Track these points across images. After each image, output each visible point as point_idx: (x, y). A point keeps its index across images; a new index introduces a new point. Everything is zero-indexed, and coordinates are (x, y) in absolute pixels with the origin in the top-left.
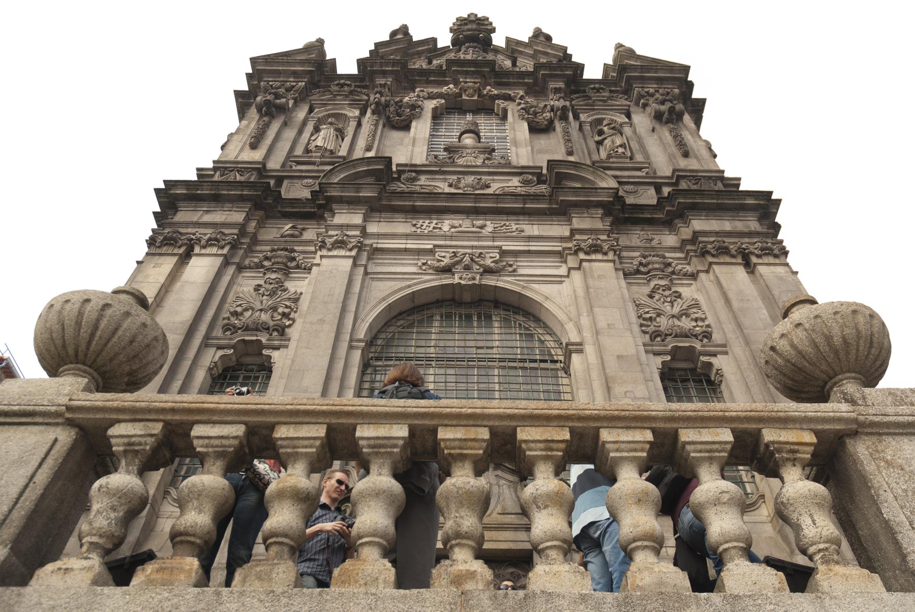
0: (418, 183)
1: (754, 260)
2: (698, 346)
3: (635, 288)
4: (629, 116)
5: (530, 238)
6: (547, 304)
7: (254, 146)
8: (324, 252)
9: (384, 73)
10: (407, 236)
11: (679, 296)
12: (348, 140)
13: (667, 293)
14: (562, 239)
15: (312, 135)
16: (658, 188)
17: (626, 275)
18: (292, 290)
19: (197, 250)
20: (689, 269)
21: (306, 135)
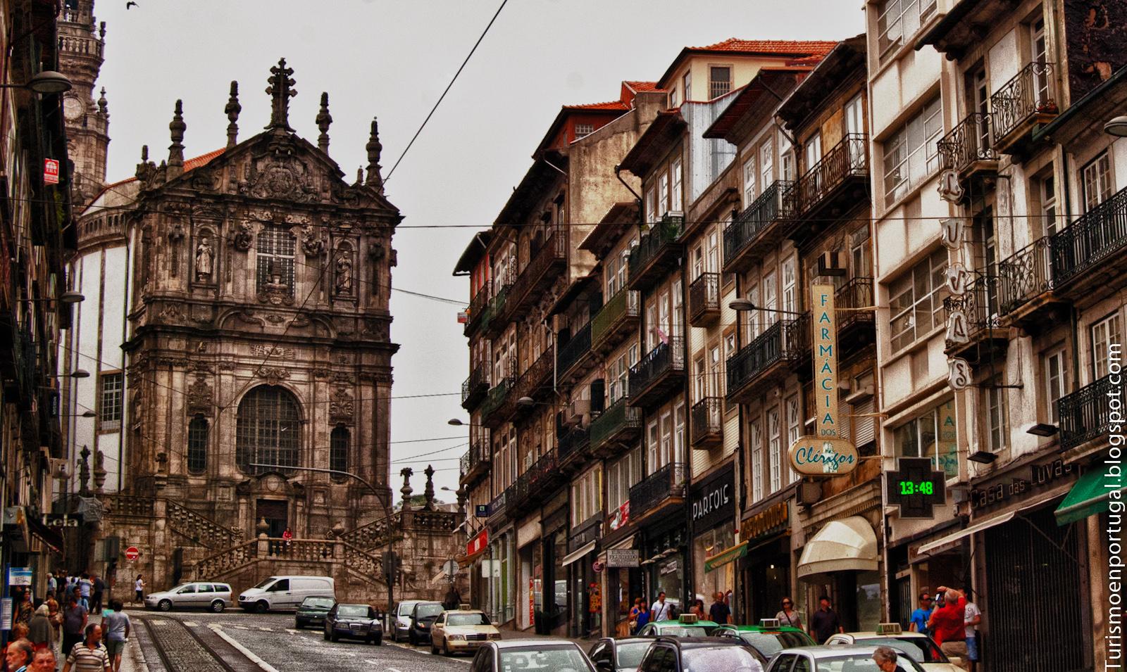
0: (254, 316)
1: (378, 384)
2: (346, 423)
3: (332, 389)
4: (358, 239)
5: (298, 361)
6: (300, 398)
7: (174, 276)
8: (222, 372)
9: (233, 203)
10: (250, 357)
11: (346, 394)
12: (215, 260)
13: (343, 394)
14: (309, 362)
15: (197, 256)
16: (356, 319)
17: (330, 382)
18: (209, 384)
19: (174, 368)
20: (353, 381)
21: (194, 256)
